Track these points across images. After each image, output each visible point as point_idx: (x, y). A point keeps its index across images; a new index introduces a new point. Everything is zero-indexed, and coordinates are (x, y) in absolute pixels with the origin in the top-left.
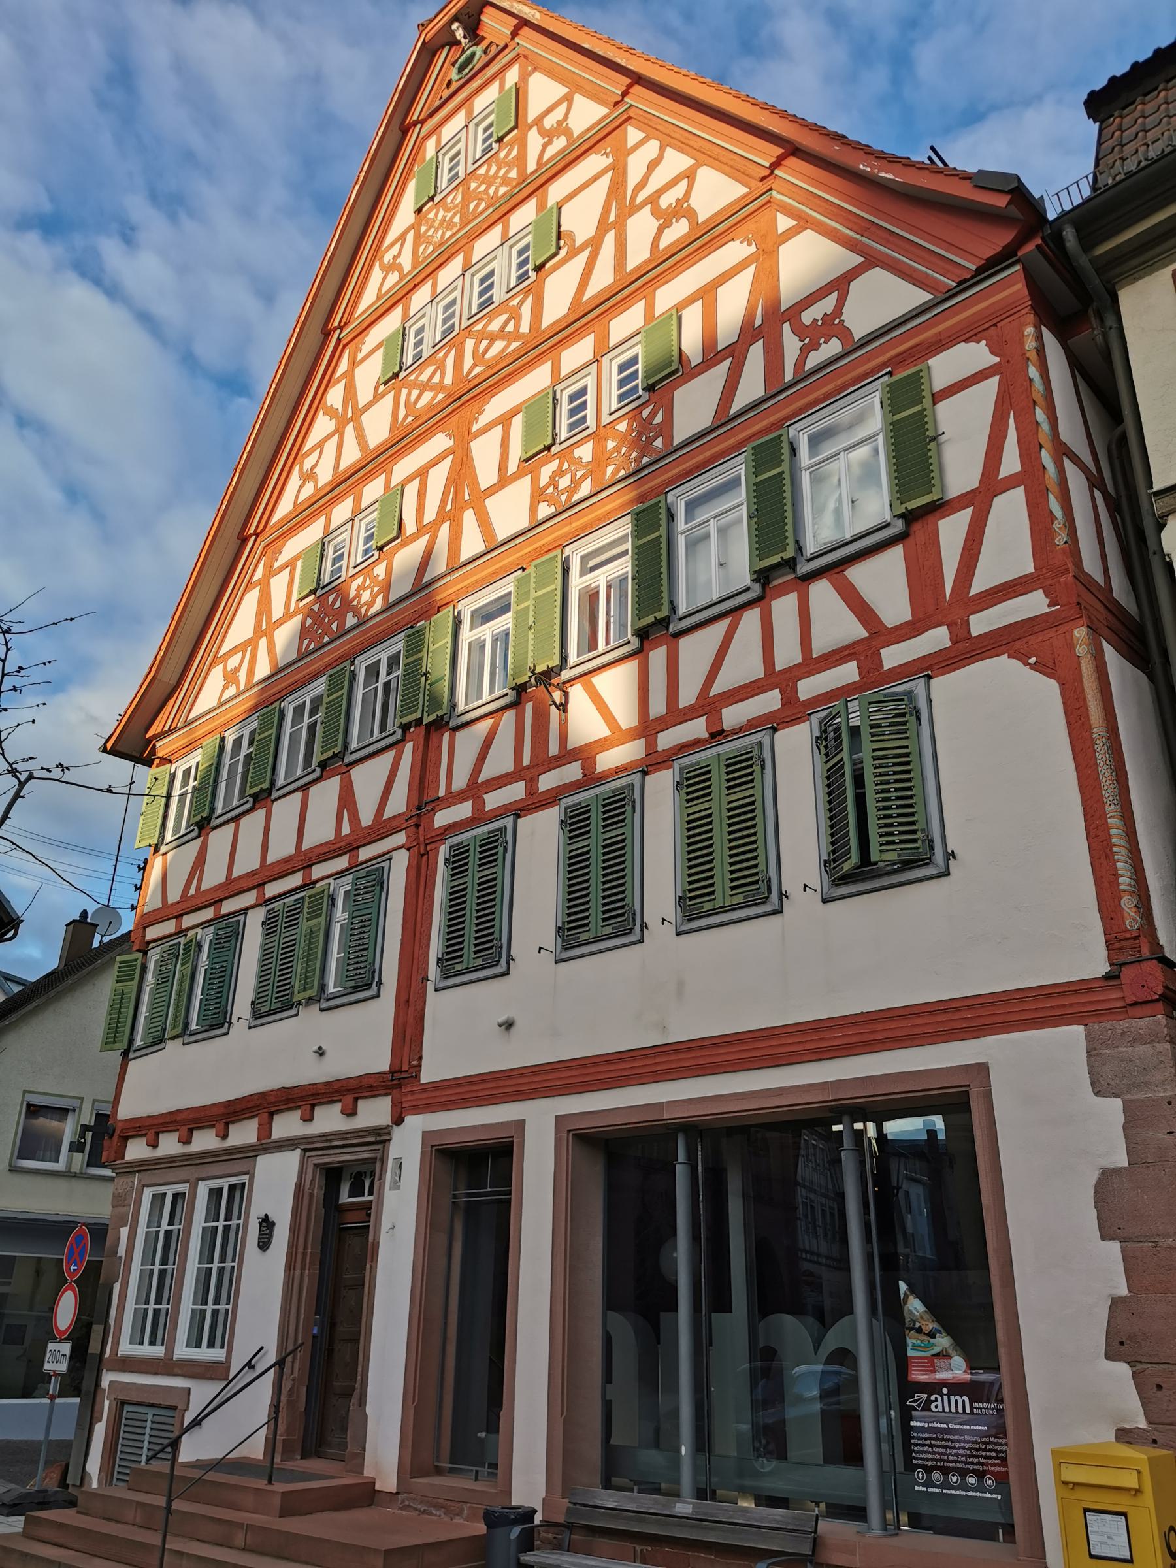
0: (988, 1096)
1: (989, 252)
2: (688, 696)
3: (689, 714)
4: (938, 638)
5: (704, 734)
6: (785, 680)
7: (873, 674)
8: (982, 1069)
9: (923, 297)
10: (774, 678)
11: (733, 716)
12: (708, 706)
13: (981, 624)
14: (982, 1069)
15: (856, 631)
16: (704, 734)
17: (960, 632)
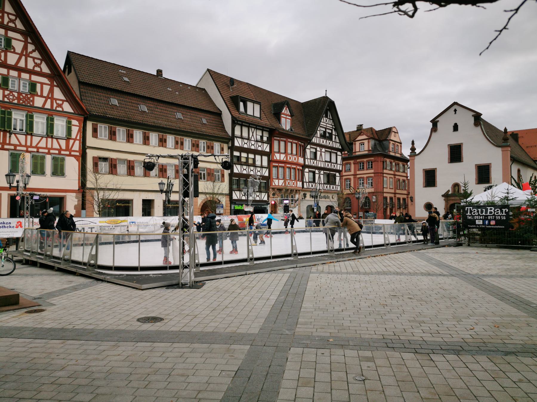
0: (66, 198)
1: (82, 114)
2: (34, 144)
3: (33, 147)
4: (68, 153)
5: (36, 151)
6: (49, 149)
7: (59, 153)
8: (66, 196)
9: (73, 112)
10: (46, 148)
11: (40, 150)
12: (36, 147)
13: (73, 153)
14: (66, 196)
15: (58, 147)
16: (36, 151)
17: (70, 153)
